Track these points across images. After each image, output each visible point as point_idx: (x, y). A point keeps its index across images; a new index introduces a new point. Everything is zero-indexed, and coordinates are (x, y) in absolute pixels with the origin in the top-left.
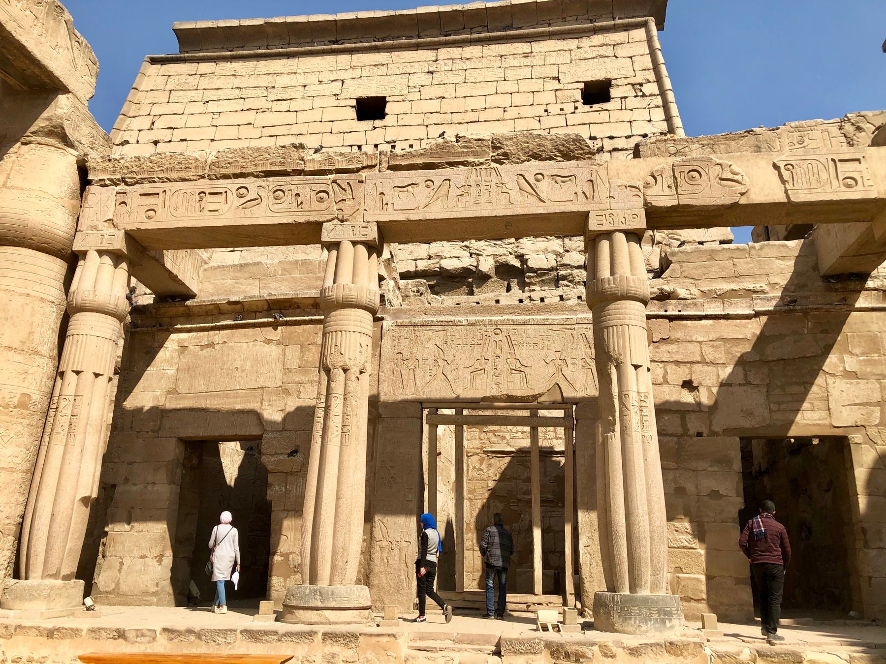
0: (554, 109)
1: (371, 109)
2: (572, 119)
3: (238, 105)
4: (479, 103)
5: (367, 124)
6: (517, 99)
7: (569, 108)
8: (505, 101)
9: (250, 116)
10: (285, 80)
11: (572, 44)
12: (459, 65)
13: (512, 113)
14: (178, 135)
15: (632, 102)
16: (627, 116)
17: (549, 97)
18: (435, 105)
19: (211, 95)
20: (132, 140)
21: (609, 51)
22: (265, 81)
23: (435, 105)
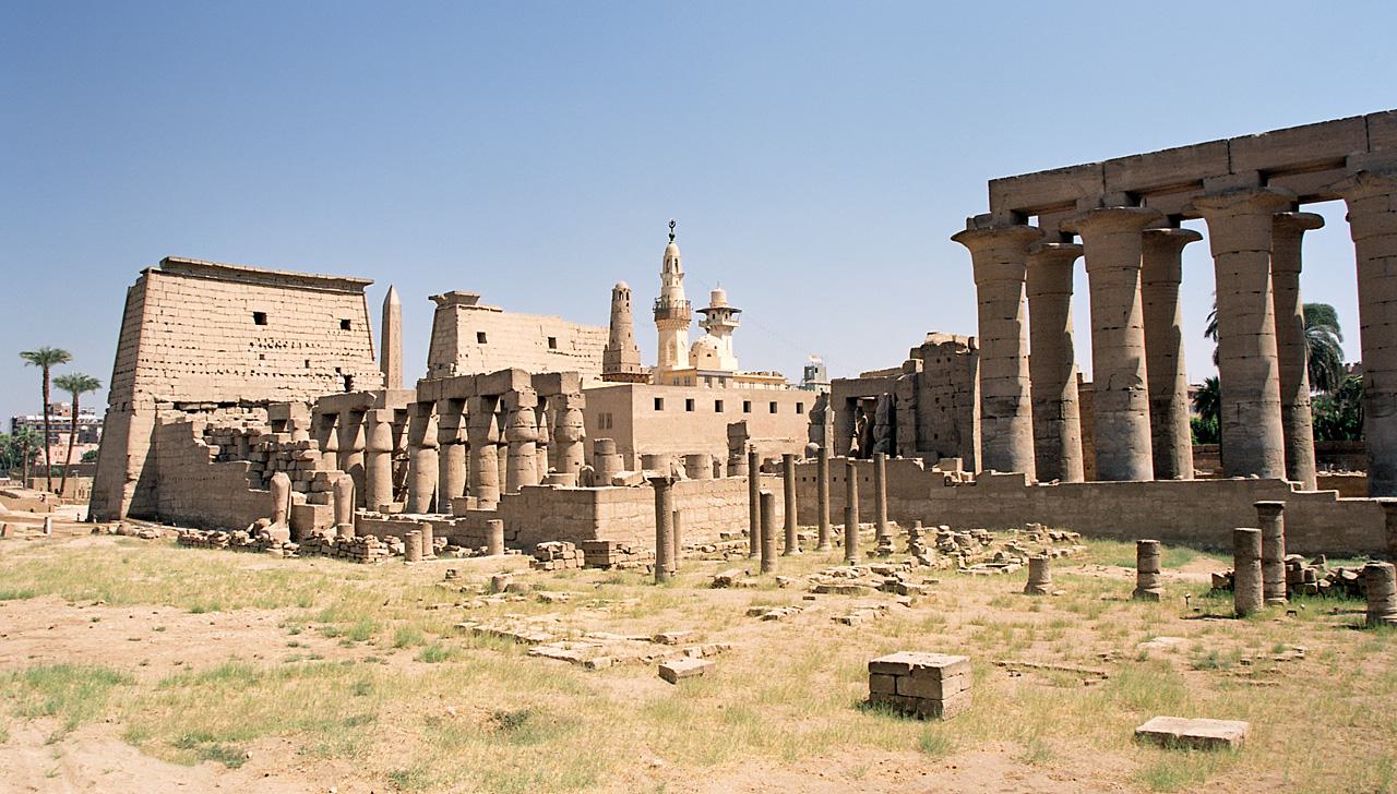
0: (331, 332)
1: (260, 318)
2: (339, 338)
3: (201, 307)
4: (304, 324)
5: (260, 327)
6: (319, 324)
7: (337, 333)
8: (313, 324)
9: (208, 315)
10: (219, 295)
11: (335, 297)
12: (294, 300)
13: (316, 331)
14: (177, 321)
15: (358, 333)
16: (356, 339)
17: (328, 325)
18: (286, 321)
19: (186, 298)
20: (154, 320)
21: (349, 304)
22: (211, 294)
23: (286, 321)
